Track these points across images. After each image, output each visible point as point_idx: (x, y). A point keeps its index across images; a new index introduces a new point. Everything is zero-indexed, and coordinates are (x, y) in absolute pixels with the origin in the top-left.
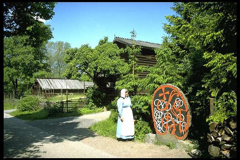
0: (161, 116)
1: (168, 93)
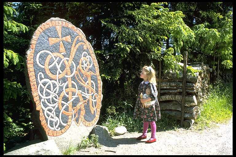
0: (57, 92)
1: (68, 38)
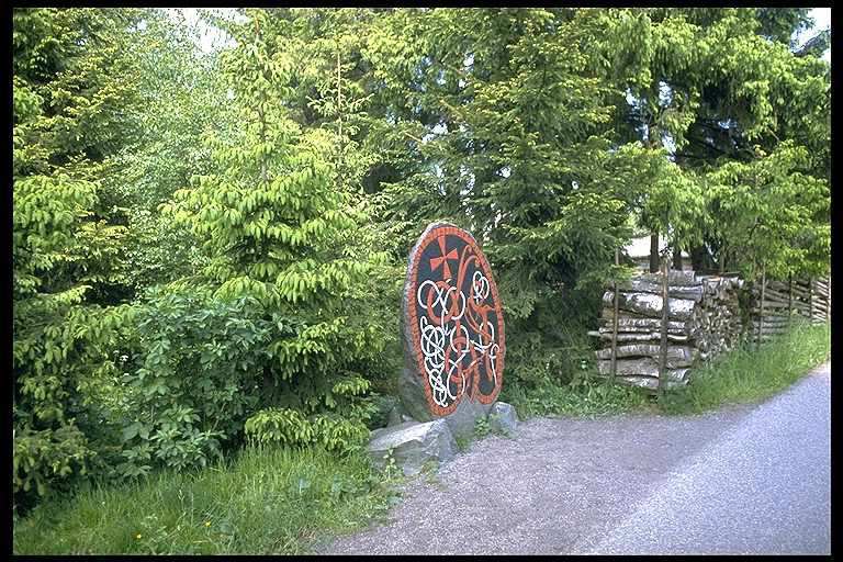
1: (454, 254)
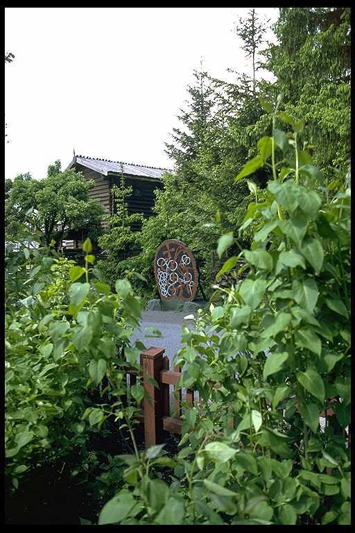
1: (173, 250)
